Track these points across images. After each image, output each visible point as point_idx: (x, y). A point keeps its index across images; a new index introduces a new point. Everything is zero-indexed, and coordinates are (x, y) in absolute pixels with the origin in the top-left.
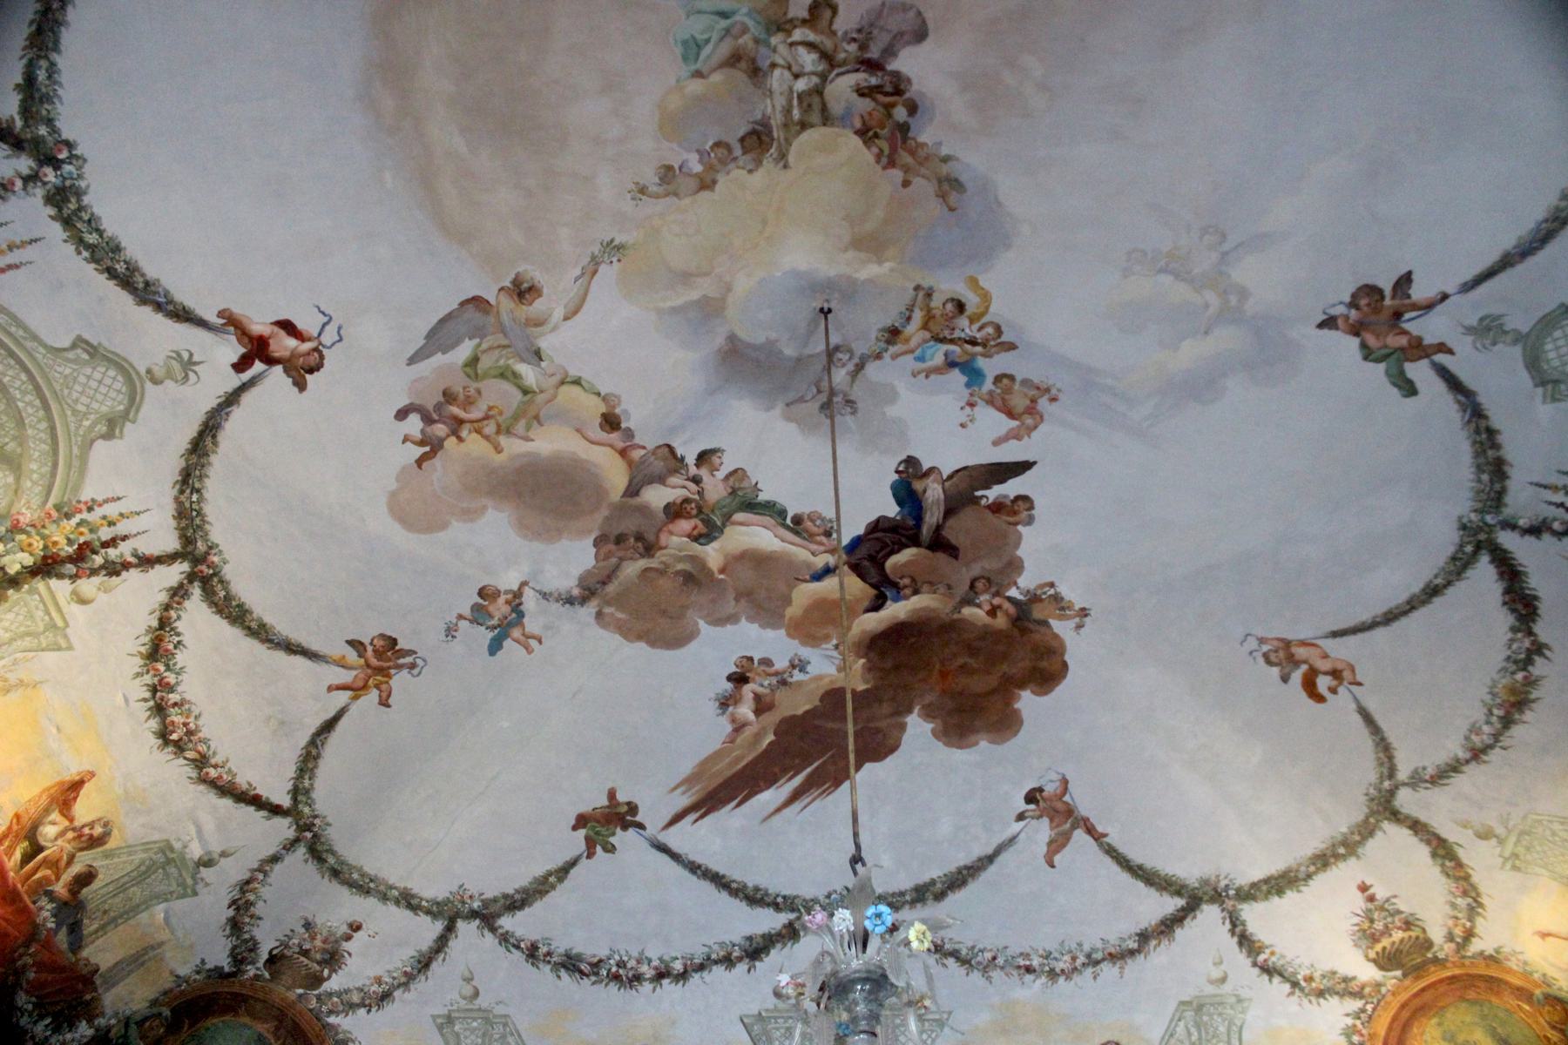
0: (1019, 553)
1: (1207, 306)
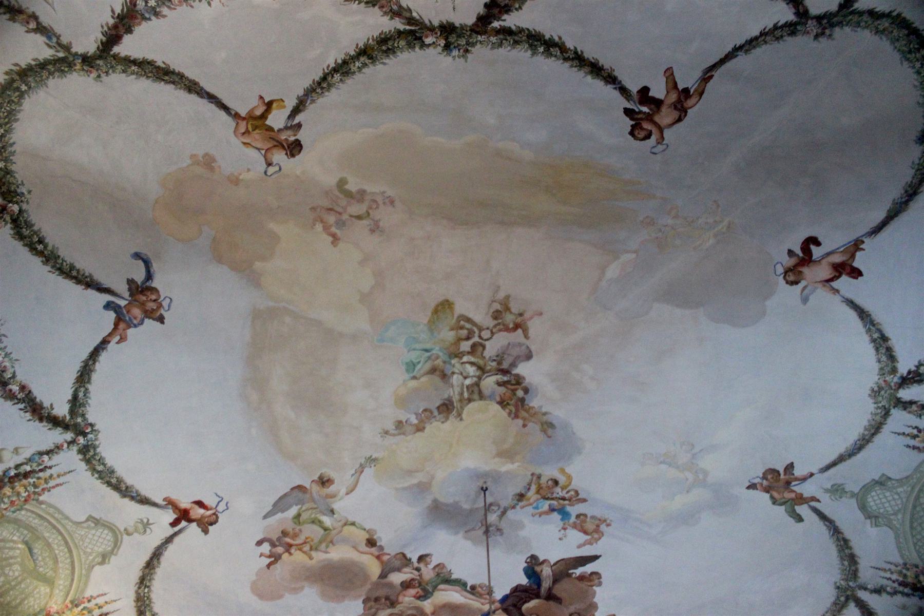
0: (595, 600)
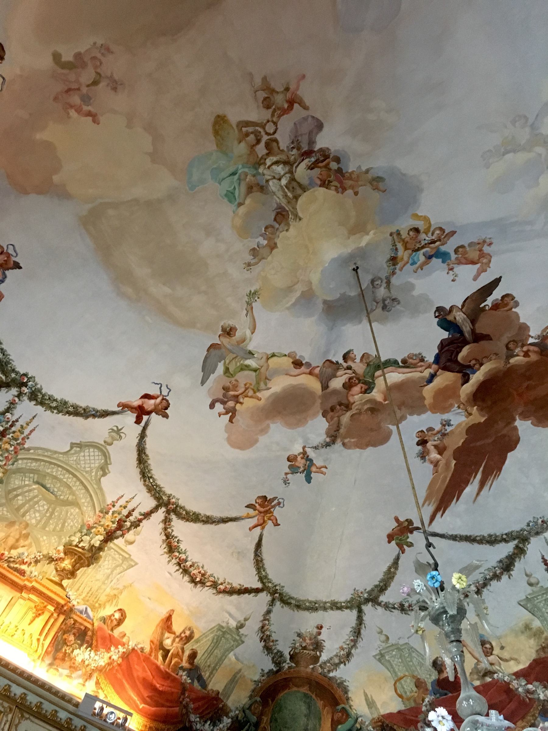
0: (522, 321)
1: (540, 155)
